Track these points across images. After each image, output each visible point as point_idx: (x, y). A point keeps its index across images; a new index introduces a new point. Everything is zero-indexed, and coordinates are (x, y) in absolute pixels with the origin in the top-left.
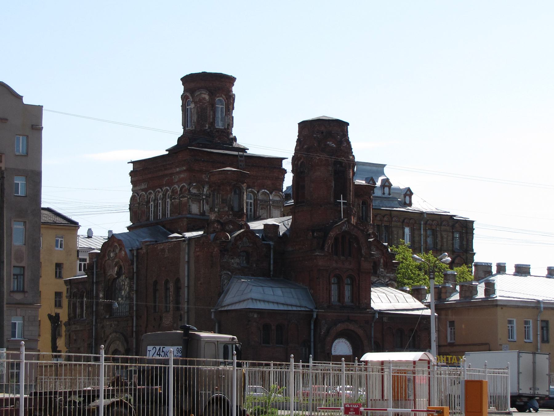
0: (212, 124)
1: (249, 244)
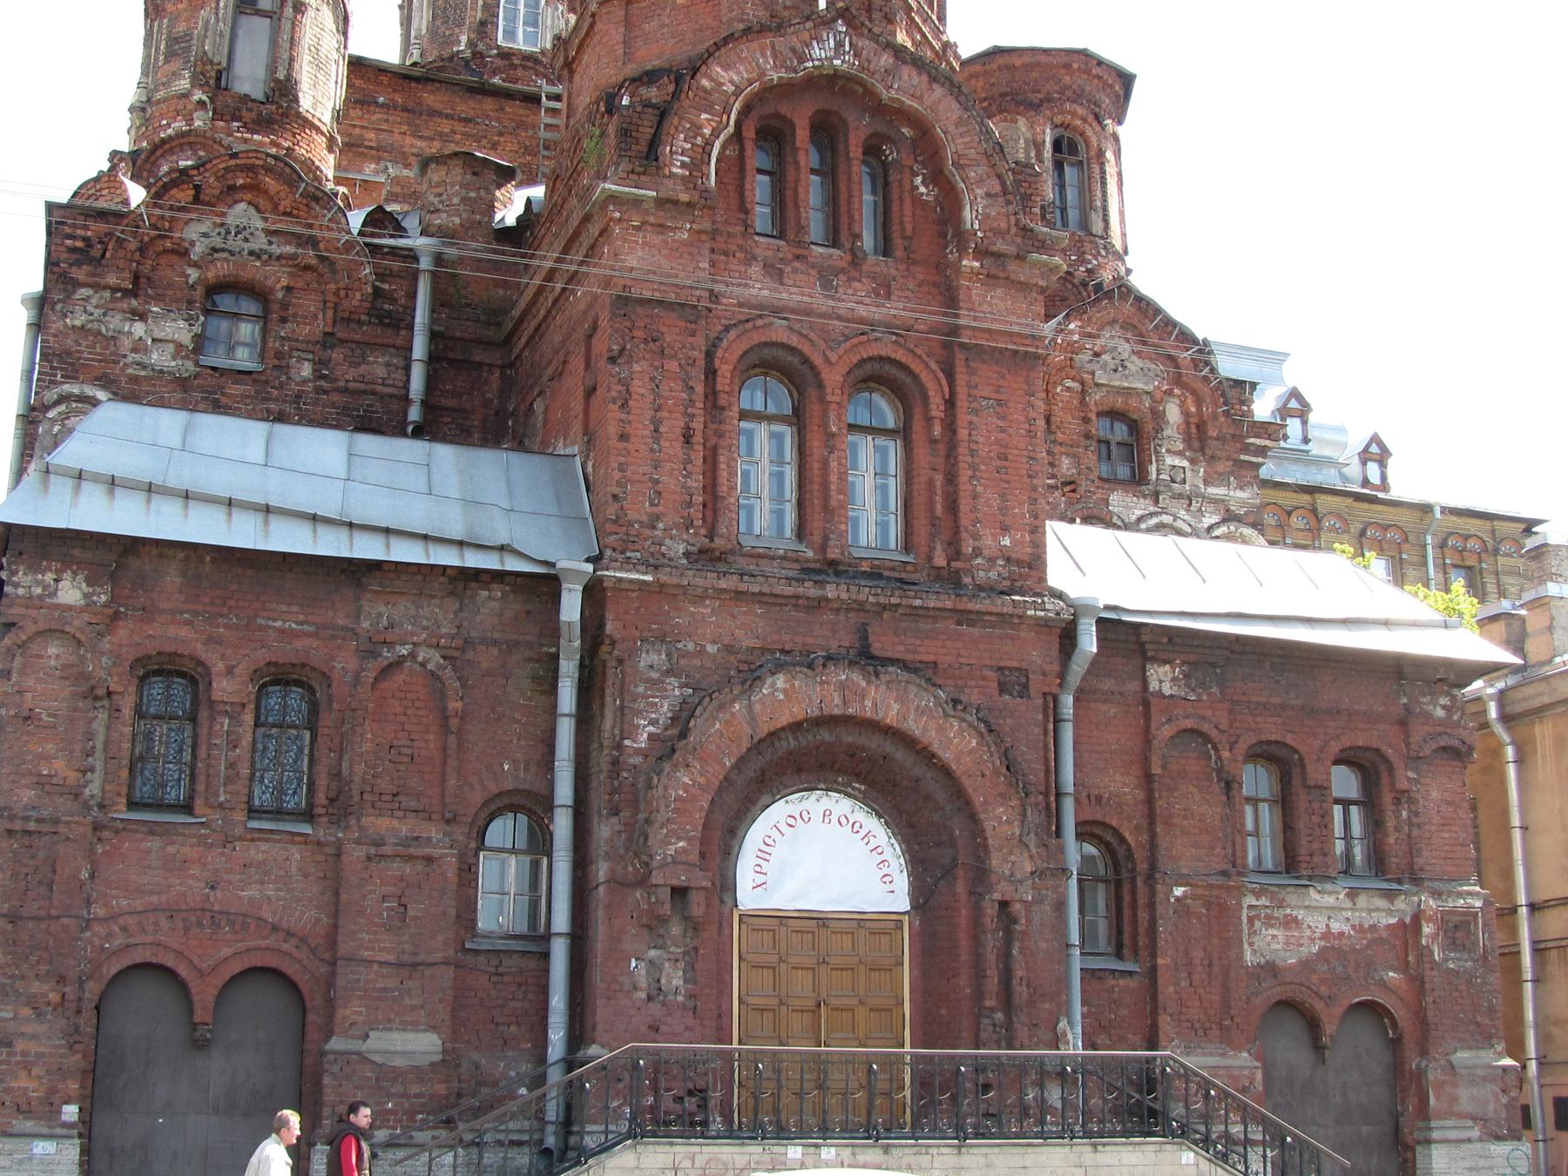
0: (485, 27)
1: (270, 243)
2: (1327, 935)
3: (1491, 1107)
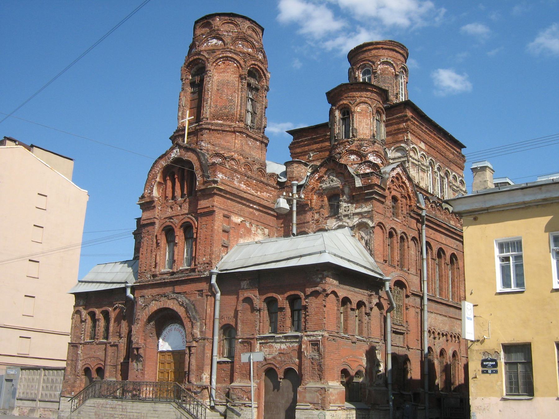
2: (280, 349)
3: (316, 399)
